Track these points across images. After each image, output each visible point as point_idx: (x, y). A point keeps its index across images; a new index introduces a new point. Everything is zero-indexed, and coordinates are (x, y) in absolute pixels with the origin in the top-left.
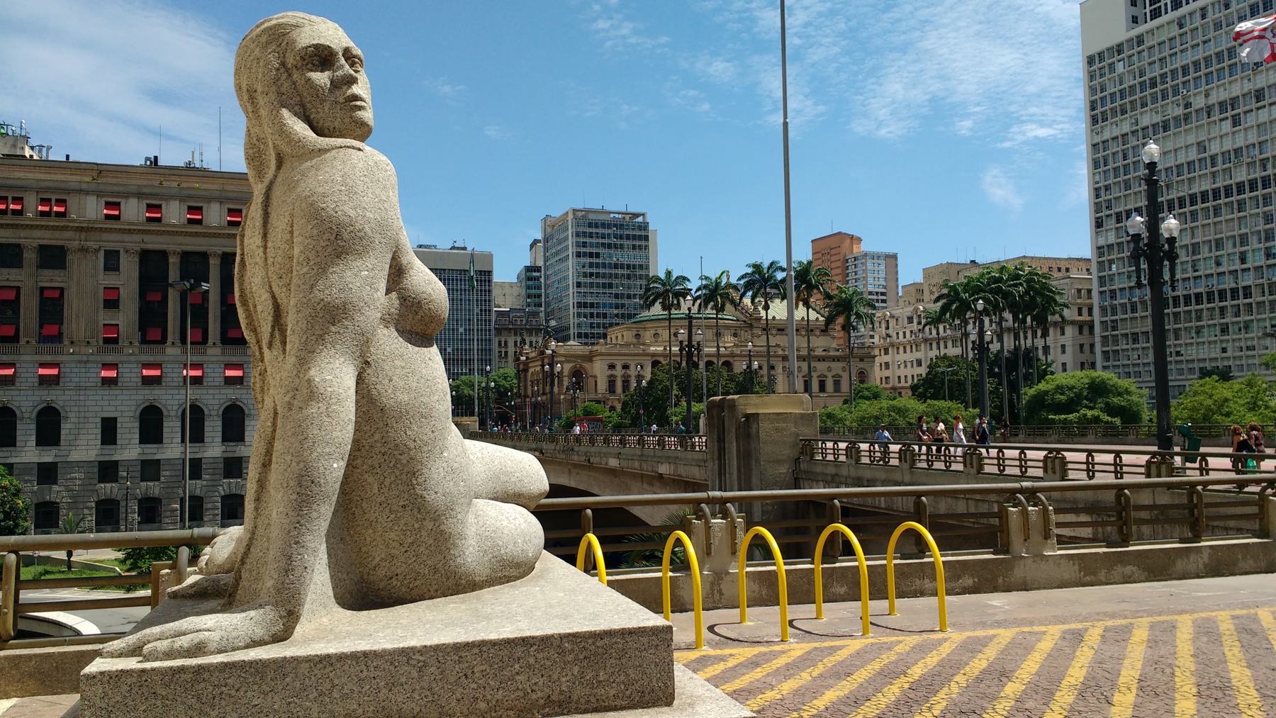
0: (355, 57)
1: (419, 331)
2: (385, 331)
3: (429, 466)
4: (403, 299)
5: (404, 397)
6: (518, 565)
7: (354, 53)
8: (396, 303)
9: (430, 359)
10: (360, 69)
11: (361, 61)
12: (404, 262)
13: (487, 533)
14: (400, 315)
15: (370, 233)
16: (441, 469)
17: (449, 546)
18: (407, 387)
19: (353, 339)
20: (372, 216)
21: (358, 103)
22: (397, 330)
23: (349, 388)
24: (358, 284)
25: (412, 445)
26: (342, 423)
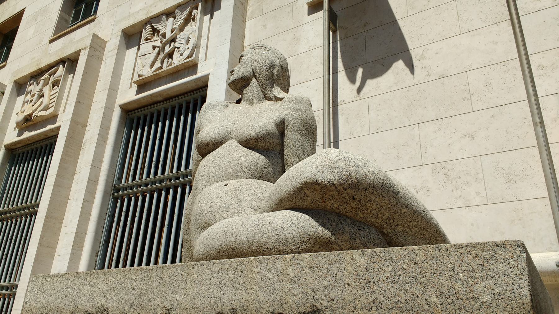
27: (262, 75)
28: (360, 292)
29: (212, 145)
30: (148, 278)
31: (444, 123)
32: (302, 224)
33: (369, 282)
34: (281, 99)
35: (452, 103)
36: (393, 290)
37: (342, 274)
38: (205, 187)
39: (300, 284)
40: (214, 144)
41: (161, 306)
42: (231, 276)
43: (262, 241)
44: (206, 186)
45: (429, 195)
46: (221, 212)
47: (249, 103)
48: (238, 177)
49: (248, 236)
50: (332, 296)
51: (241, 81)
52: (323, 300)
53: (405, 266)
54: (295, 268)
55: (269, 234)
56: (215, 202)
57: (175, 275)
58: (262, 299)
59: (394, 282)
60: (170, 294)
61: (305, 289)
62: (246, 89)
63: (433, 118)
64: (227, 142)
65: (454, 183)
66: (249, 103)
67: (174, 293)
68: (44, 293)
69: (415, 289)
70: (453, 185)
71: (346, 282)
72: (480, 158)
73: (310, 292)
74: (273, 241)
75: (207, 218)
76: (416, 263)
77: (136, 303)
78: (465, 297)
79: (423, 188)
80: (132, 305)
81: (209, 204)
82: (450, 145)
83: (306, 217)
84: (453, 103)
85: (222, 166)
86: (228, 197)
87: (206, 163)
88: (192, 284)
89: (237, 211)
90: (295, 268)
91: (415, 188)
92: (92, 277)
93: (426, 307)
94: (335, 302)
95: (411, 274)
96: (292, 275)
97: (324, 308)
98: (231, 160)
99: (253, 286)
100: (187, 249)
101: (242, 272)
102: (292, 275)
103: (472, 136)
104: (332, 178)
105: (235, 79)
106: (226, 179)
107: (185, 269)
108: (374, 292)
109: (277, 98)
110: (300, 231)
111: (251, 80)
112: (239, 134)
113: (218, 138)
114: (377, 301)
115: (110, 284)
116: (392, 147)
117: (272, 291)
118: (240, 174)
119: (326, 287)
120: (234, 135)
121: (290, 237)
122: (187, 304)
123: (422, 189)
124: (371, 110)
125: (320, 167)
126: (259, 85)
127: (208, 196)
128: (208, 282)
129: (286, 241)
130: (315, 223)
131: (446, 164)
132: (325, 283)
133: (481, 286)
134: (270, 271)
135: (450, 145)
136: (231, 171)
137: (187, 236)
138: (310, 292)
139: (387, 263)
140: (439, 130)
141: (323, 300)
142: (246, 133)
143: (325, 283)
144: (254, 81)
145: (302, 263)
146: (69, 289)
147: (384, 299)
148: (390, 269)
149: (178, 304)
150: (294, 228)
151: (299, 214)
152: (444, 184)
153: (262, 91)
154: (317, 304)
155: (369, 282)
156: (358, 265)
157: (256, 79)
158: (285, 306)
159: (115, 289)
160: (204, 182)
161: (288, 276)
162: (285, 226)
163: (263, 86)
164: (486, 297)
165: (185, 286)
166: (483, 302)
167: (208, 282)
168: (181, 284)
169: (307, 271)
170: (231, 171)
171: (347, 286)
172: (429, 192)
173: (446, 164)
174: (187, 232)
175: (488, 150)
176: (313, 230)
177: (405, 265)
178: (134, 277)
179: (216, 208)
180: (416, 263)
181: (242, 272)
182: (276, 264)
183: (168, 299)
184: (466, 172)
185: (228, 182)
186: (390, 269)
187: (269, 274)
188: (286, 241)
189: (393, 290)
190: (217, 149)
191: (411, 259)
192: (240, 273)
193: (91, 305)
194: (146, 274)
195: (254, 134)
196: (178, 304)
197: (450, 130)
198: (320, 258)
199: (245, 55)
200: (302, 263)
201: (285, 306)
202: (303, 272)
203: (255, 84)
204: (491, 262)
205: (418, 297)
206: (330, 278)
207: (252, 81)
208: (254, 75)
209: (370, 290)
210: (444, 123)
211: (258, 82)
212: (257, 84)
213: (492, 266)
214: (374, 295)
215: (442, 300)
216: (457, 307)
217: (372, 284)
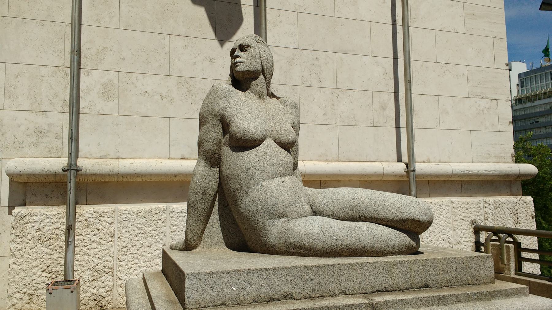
0: (244, 46)
1: (238, 146)
2: (227, 148)
3: (241, 199)
4: (229, 135)
5: (228, 172)
6: (306, 249)
7: (243, 45)
8: (228, 137)
9: (241, 156)
10: (247, 49)
11: (247, 46)
12: (228, 121)
13: (284, 230)
14: (230, 141)
15: (206, 116)
16: (247, 200)
17: (258, 232)
18: (229, 168)
19: (203, 153)
20: (206, 110)
21: (237, 64)
22: (230, 147)
23: (199, 171)
24: (203, 135)
25: (232, 190)
26: (194, 182)
27: (269, 74)
28: (444, 276)
29: (258, 141)
30: (323, 272)
31: (192, 42)
32: (402, 239)
33: (447, 272)
34: (278, 98)
35: (200, 25)
36: (456, 274)
37: (437, 268)
38: (263, 180)
39: (419, 274)
40: (259, 141)
41: (337, 289)
42: (382, 270)
43: (380, 246)
44: (264, 180)
45: (172, 104)
46: (292, 207)
47: (258, 96)
48: (286, 175)
49: (370, 242)
50: (433, 278)
51: (251, 74)
52: (429, 280)
53: (460, 265)
54: (416, 266)
55: (384, 242)
56: (286, 198)
57: (343, 270)
58: (400, 282)
59: (456, 271)
60: (342, 282)
61: (421, 276)
62: (254, 82)
63: (183, 34)
64: (266, 140)
65: (194, 97)
66: (258, 96)
67: (345, 281)
68: (211, 287)
69: (463, 274)
70: (193, 99)
71: (439, 272)
72: (216, 81)
73: (424, 277)
74: (387, 247)
75: (281, 210)
76: (464, 264)
77: (317, 288)
78: (478, 276)
79: (168, 96)
80: (313, 290)
81: (281, 199)
82: (194, 63)
83: (403, 235)
84: (201, 26)
85: (274, 164)
86: (292, 195)
87: (258, 158)
88: (358, 275)
89: (300, 206)
90: (416, 266)
91: (161, 94)
92: (268, 273)
93: (466, 280)
94: (434, 281)
95: (462, 268)
96: (415, 269)
97: (430, 284)
98: (279, 160)
99: (395, 275)
100: (198, 214)
101: (388, 268)
102: (415, 269)
103: (212, 62)
104: (426, 219)
105: (247, 70)
106: (279, 175)
107: (350, 266)
108: (449, 276)
109: (274, 95)
110: (402, 242)
111: (260, 75)
112: (277, 136)
113: (262, 136)
114: (450, 280)
115: (288, 277)
116: (142, 50)
117: (405, 278)
118: (287, 172)
119: (430, 275)
120: (269, 134)
121: (396, 245)
122: (356, 287)
123: (166, 98)
124: (122, 3)
125: (421, 212)
126: (266, 82)
127: (275, 191)
128: (368, 274)
129: (394, 247)
130: (409, 238)
131: (189, 79)
132: (430, 273)
133: (482, 272)
134: (403, 267)
135: (194, 63)
136: (281, 169)
137: (200, 204)
138: (424, 277)
139: (454, 264)
140: (187, 47)
141: (429, 280)
142: (285, 137)
143: (430, 273)
144: (261, 76)
145: (419, 264)
146: (244, 283)
147: (453, 278)
148: (455, 266)
149: (350, 287)
150: (398, 240)
151: (398, 232)
152: (186, 97)
153: (267, 87)
154: (427, 283)
155: (447, 272)
156: (443, 264)
157: (264, 76)
158: (412, 284)
159: (295, 280)
160: (261, 176)
161: (412, 270)
162: (393, 239)
163: (268, 84)
164: (483, 276)
165: (352, 277)
166: (483, 277)
167: (368, 274)
168: (350, 276)
169: (421, 267)
170: (281, 169)
171: (439, 274)
172: (172, 101)
173: (189, 79)
174: (201, 201)
175: (222, 76)
176: (408, 242)
177: (460, 264)
178: (310, 272)
179: (287, 203)
180: (464, 264)
181: (388, 268)
182: (406, 264)
183: (342, 284)
184: (204, 91)
185: (283, 179)
186: (455, 266)
187: (403, 269)
188: (394, 247)
189: (456, 274)
190: (261, 145)
191: (462, 262)
192: (387, 269)
193: (274, 293)
194: (320, 270)
195: (292, 140)
196: (350, 287)
197: (195, 50)
198: (427, 261)
199: (253, 47)
200: (419, 264)
201: (412, 284)
202: (420, 268)
203: (263, 80)
204: (486, 263)
205: (464, 277)
206: (432, 270)
207: (260, 76)
208: (263, 71)
209: (448, 275)
210: (192, 42)
211: (265, 79)
212: (265, 81)
213: (486, 265)
214: (449, 277)
215: (472, 278)
216: (476, 280)
217: (448, 273)
